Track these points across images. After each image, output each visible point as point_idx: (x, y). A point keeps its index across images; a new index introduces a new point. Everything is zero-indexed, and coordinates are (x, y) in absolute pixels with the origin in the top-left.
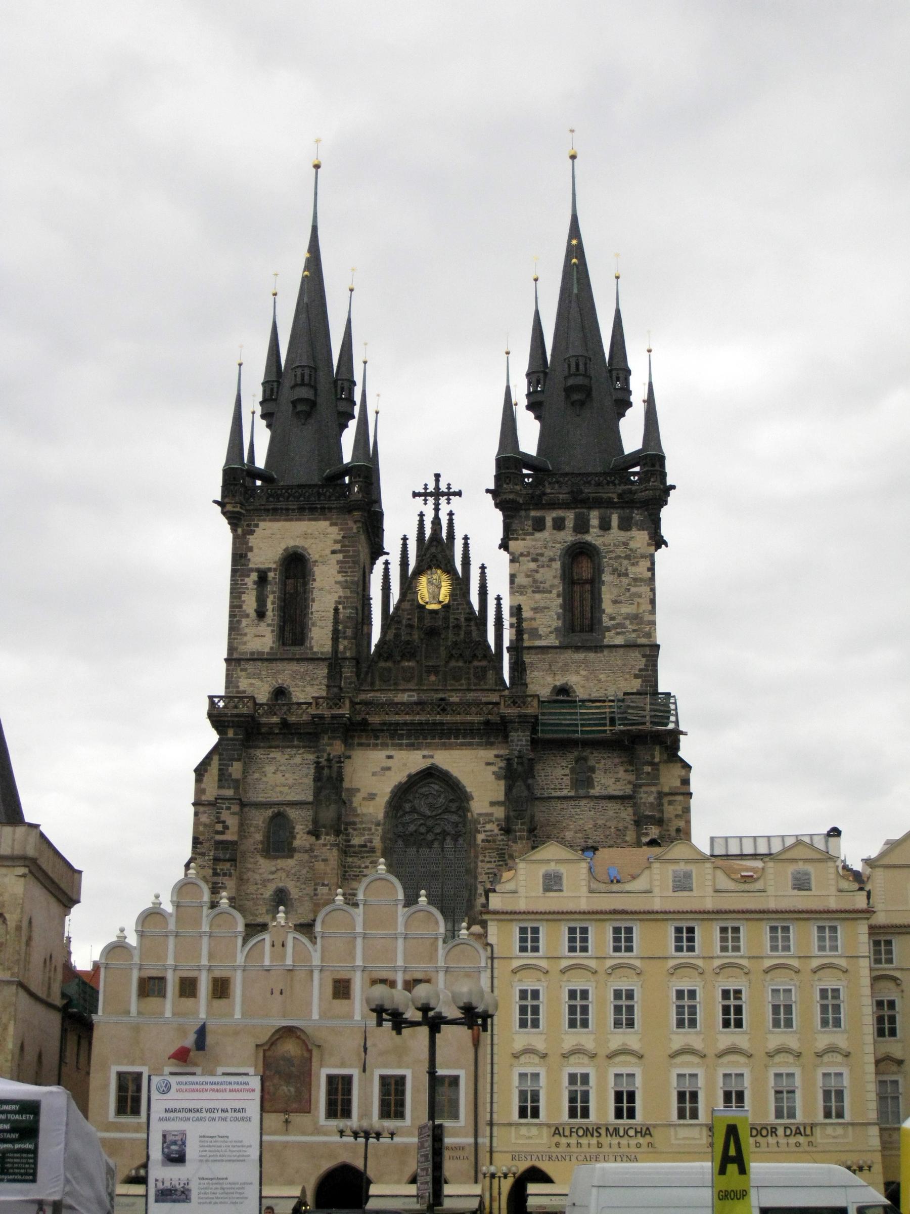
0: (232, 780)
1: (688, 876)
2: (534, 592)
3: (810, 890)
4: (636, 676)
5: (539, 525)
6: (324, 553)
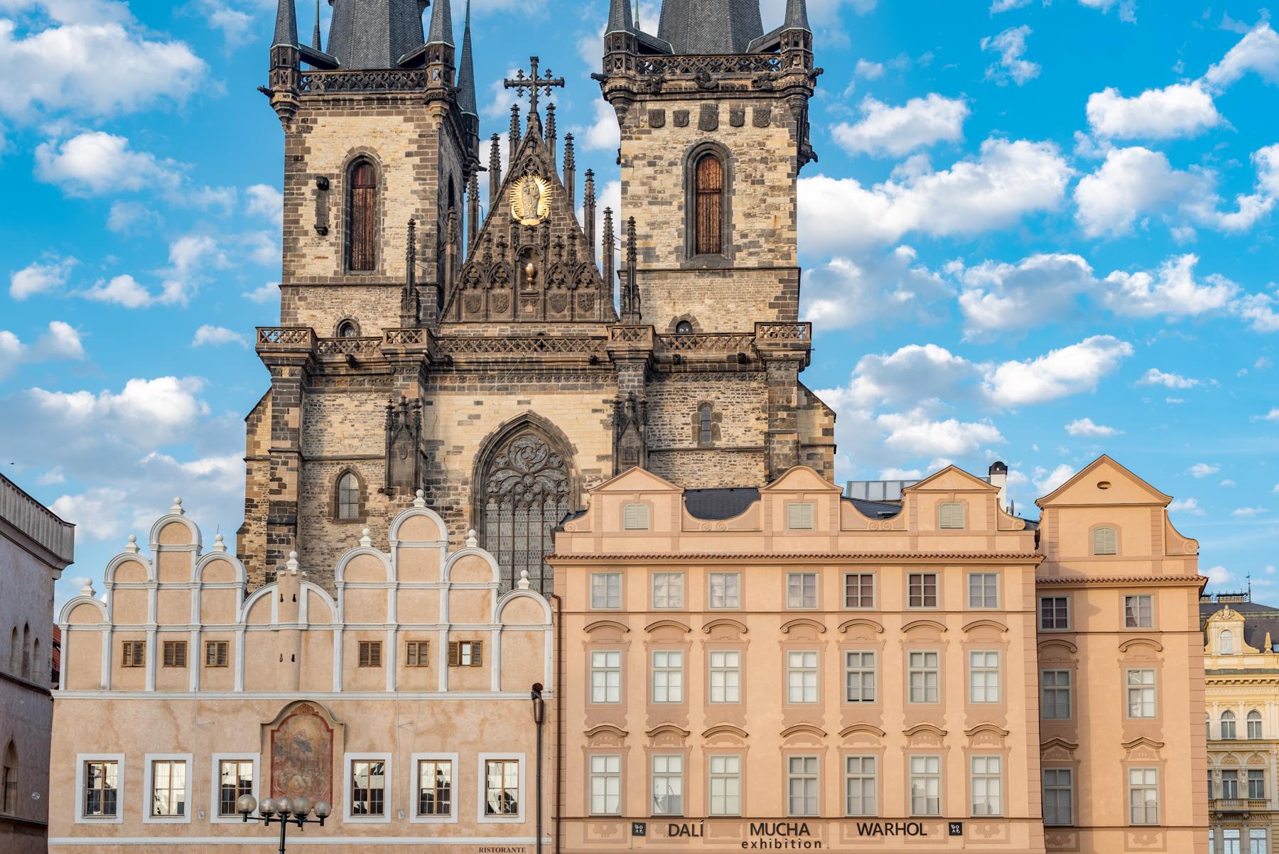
2: (650, 203)
4: (771, 306)
5: (657, 120)
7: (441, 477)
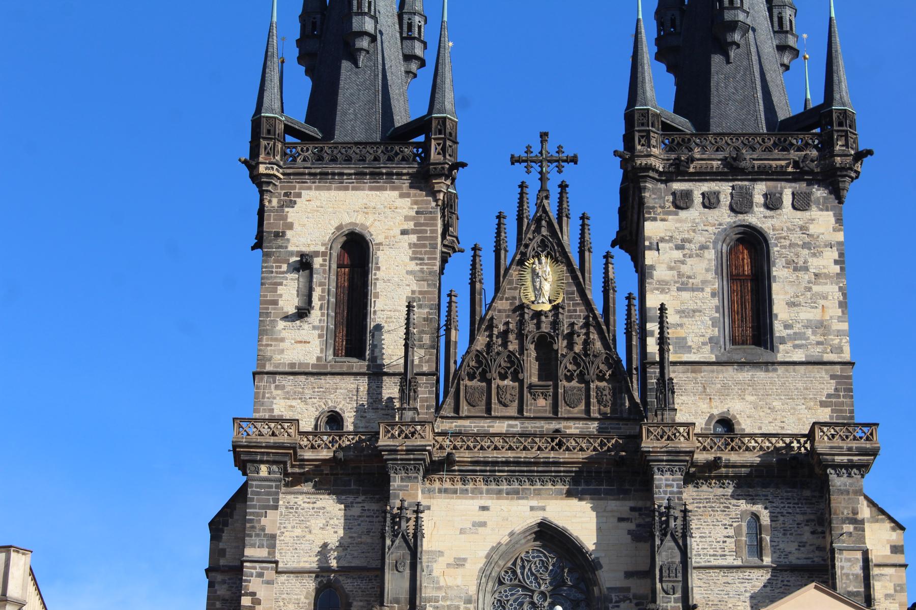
0: (265, 535)
2: (679, 289)
4: (823, 404)
6: (392, 233)
7: (441, 594)
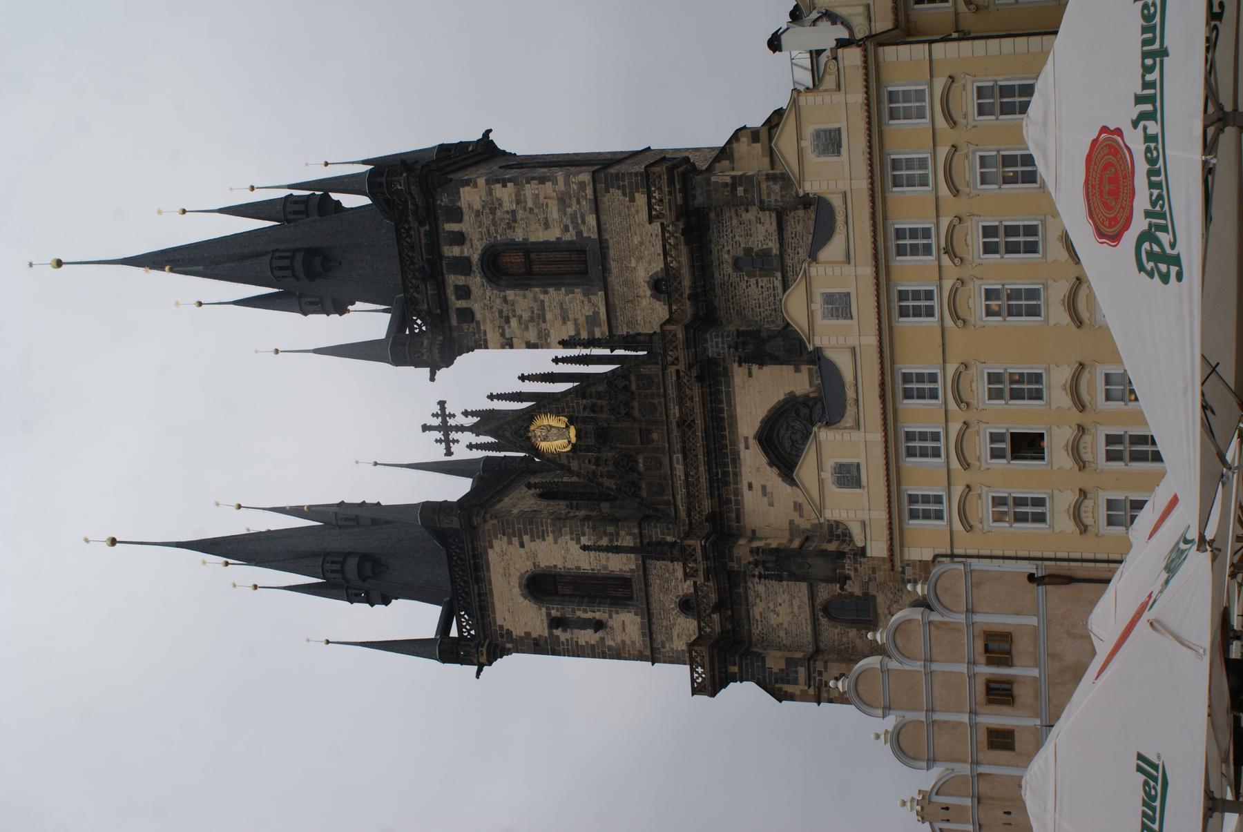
1: (829, 298)
2: (544, 321)
3: (839, 130)
4: (632, 200)
5: (467, 315)
